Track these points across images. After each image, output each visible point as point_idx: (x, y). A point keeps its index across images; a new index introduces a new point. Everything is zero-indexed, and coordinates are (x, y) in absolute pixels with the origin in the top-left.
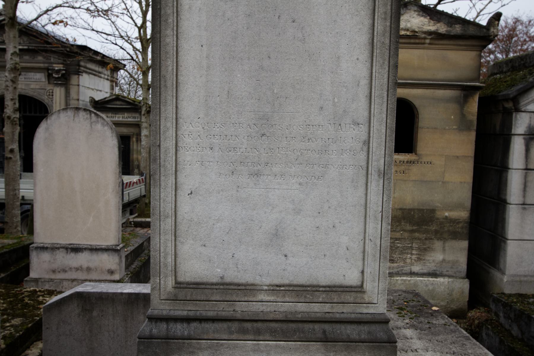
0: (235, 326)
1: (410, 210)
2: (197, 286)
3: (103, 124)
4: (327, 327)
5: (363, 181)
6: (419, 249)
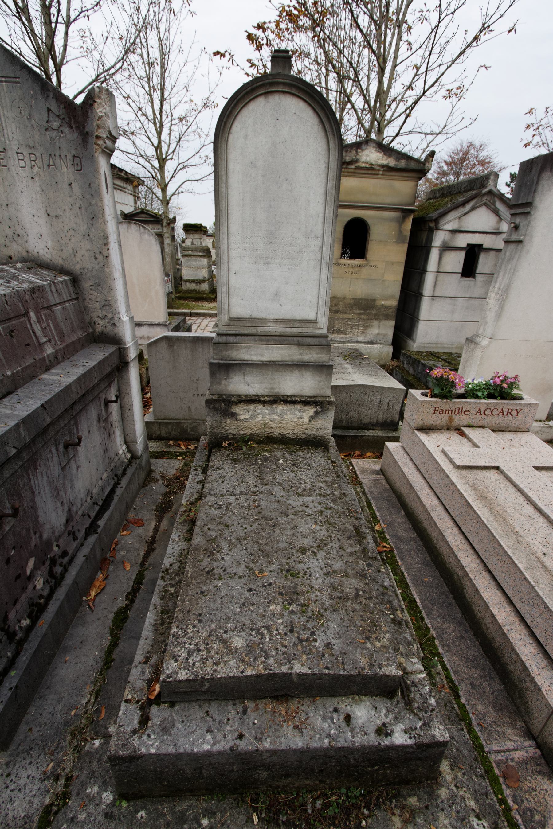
0: (257, 338)
1: (359, 299)
2: (239, 319)
3: (149, 235)
4: (299, 339)
5: (319, 267)
6: (363, 326)
